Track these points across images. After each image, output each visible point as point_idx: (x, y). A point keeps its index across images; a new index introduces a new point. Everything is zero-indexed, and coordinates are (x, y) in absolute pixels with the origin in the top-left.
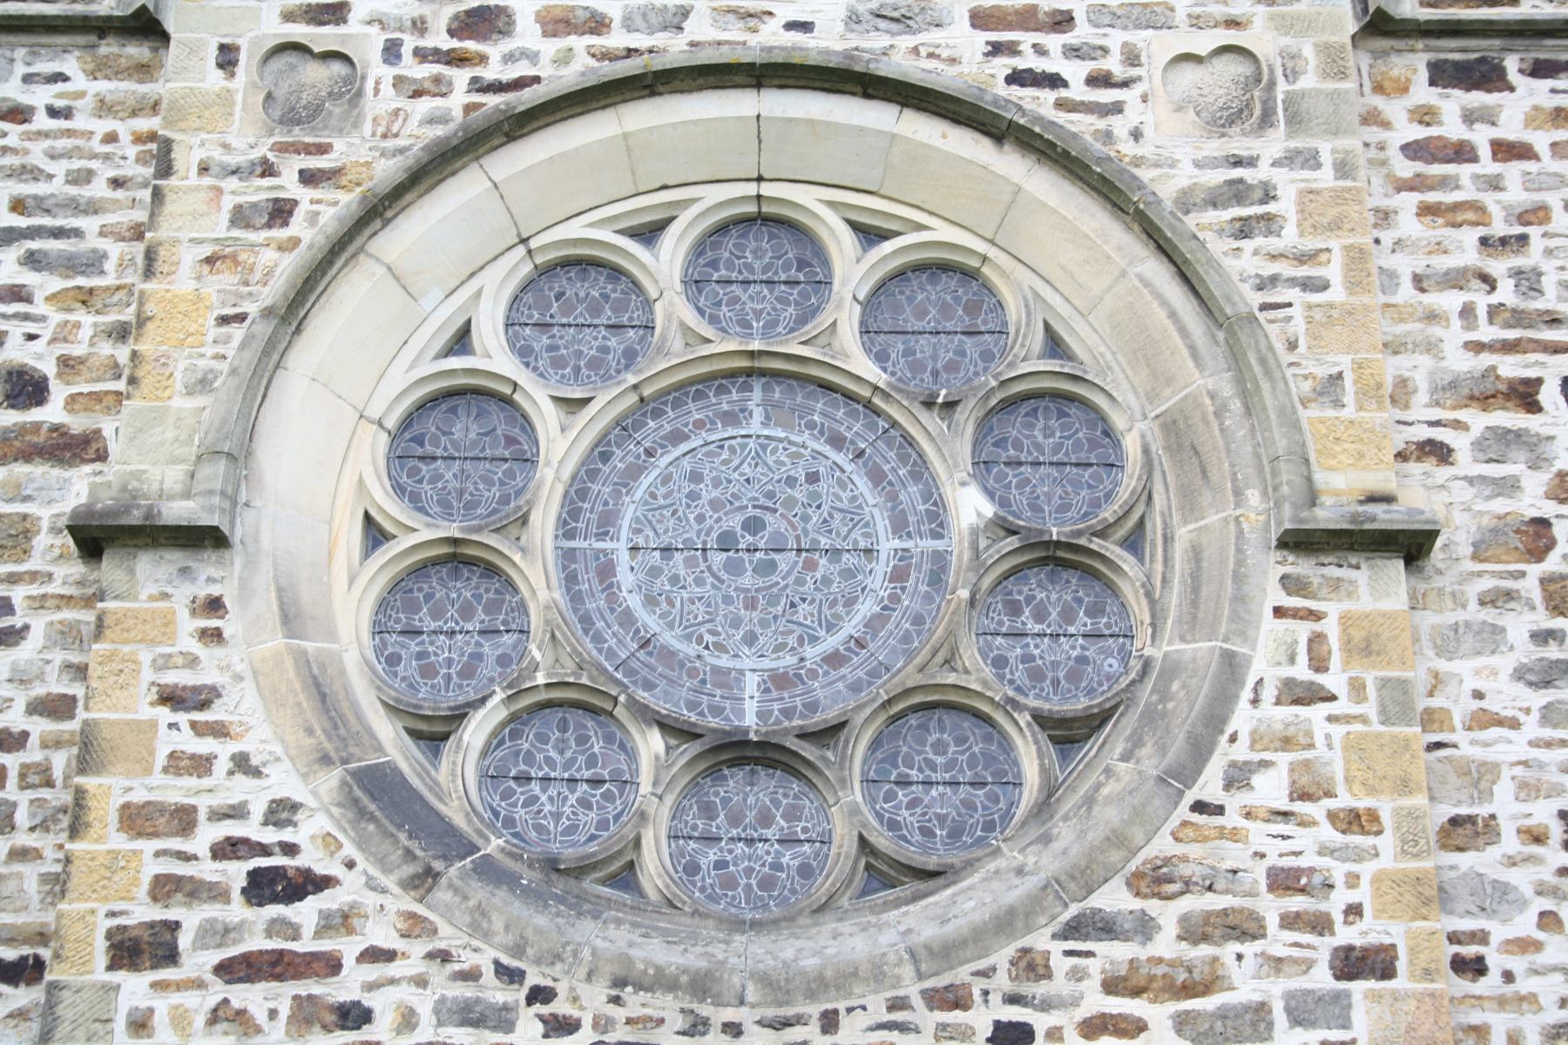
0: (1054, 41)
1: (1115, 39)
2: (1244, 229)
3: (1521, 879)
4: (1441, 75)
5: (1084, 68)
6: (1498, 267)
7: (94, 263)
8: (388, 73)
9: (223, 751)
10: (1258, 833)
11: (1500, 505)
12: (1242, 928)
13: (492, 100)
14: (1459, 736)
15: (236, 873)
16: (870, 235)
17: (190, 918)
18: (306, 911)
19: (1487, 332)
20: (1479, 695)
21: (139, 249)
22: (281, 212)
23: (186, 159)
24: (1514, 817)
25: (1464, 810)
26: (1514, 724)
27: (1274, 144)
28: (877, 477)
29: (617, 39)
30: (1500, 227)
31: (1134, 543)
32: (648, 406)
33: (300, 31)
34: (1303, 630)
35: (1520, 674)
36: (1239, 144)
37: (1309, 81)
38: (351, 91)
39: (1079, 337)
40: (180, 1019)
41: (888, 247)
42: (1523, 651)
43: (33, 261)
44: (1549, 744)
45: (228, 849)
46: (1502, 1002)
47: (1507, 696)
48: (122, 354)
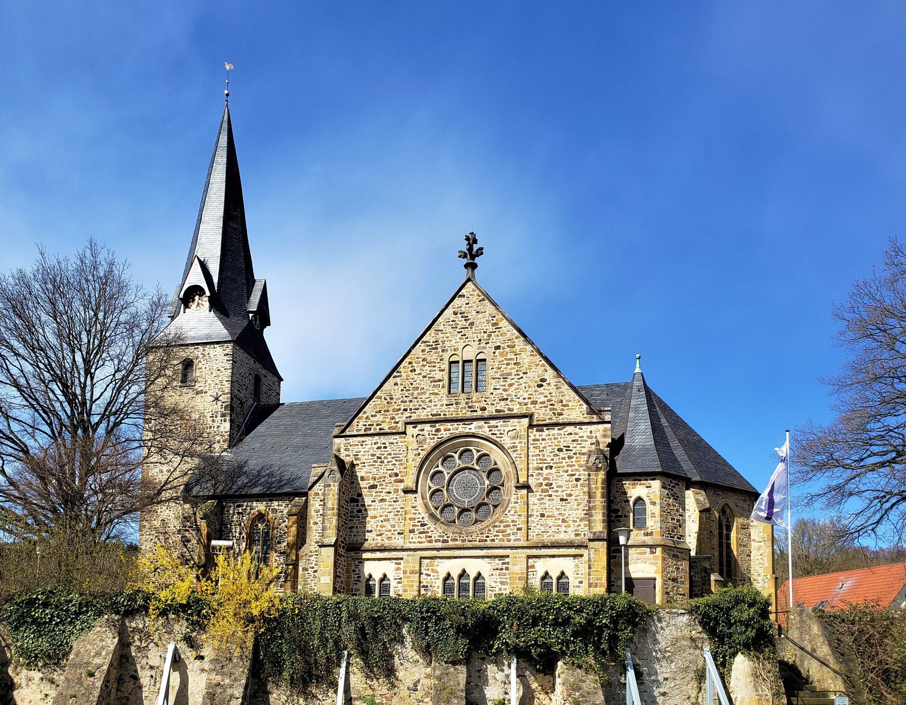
0: (496, 429)
1: (502, 428)
2: (514, 451)
4: (537, 431)
5: (499, 432)
6: (540, 454)
7: (402, 460)
8: (428, 437)
9: (417, 512)
10: (511, 517)
11: (538, 481)
13: (440, 440)
15: (419, 524)
16: (478, 451)
17: (416, 528)
18: (426, 527)
19: (539, 462)
21: (406, 459)
22: (419, 454)
27: (518, 441)
28: (478, 479)
29: (452, 431)
30: (541, 449)
31: (503, 486)
33: (420, 432)
34: (516, 496)
35: (538, 499)
36: (514, 441)
37: (522, 433)
38: (425, 440)
39: (498, 462)
40: (415, 538)
41: (479, 453)
42: (538, 497)
43: (396, 460)
45: (419, 522)
47: (537, 502)
48: (405, 470)
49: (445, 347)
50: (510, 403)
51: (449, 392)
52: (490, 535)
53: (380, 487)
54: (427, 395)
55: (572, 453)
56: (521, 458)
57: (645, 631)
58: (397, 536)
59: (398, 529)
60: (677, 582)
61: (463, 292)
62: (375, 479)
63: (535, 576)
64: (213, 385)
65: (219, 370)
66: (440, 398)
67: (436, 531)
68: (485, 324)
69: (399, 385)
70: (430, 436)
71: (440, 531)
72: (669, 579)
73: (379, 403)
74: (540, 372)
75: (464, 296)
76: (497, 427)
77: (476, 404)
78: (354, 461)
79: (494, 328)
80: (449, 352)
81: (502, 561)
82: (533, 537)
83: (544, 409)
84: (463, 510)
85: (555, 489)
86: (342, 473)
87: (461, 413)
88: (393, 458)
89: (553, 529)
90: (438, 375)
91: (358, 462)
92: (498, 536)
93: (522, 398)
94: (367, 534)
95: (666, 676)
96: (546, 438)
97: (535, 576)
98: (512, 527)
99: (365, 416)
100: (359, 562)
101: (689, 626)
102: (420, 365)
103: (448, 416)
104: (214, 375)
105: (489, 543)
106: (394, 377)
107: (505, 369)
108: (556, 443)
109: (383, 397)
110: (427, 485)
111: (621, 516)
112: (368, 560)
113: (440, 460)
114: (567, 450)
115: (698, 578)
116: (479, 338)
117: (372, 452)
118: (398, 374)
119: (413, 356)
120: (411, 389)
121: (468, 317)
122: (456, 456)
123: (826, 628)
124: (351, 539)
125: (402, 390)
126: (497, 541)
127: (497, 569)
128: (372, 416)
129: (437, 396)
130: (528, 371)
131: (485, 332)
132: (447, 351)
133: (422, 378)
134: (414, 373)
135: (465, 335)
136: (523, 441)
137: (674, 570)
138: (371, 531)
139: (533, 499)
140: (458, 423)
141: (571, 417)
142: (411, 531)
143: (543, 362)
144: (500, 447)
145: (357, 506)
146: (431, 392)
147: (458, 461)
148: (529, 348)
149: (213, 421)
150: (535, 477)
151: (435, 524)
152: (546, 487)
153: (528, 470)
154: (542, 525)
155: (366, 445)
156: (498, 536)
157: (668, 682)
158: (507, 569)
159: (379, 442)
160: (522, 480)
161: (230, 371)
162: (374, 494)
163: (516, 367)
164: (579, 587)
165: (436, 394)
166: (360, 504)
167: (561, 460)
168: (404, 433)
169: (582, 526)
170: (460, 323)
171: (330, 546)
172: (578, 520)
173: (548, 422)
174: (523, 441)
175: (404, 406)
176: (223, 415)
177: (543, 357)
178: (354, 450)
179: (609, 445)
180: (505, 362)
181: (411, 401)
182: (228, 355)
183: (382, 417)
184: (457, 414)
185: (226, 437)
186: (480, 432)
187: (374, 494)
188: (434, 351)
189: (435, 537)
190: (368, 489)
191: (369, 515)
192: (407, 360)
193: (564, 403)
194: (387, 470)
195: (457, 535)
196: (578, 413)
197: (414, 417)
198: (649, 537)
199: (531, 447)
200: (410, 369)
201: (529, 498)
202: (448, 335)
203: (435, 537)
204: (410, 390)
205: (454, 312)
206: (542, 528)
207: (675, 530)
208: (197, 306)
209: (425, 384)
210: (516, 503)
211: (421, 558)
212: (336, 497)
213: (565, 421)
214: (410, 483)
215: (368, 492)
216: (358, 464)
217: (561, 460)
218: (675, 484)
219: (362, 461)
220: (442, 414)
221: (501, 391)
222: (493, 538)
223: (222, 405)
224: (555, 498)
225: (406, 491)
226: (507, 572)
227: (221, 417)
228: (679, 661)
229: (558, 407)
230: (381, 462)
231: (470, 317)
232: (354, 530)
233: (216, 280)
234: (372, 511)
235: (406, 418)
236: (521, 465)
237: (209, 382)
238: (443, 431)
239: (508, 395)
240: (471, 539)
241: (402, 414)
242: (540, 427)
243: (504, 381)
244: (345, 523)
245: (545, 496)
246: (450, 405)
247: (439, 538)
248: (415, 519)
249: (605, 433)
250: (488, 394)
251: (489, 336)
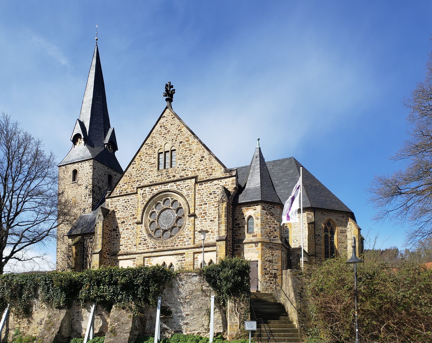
0: (179, 186)
1: (183, 185)
5: (181, 188)
6: (201, 197)
7: (136, 208)
9: (142, 234)
11: (200, 212)
12: (185, 237)
15: (143, 240)
17: (142, 242)
18: (146, 241)
19: (200, 201)
23: (139, 201)
28: (173, 214)
29: (159, 190)
30: (202, 195)
31: (184, 216)
32: (162, 211)
33: (144, 192)
34: (189, 221)
36: (188, 192)
38: (146, 196)
41: (173, 200)
42: (200, 220)
43: (133, 208)
45: (143, 239)
47: (199, 223)
49: (156, 145)
50: (187, 172)
51: (158, 169)
52: (176, 243)
53: (126, 222)
54: (148, 172)
55: (216, 195)
56: (191, 200)
57: (171, 286)
58: (134, 247)
59: (134, 243)
60: (272, 263)
61: (165, 114)
62: (124, 218)
63: (197, 263)
64: (85, 181)
65: (87, 173)
66: (154, 173)
67: (151, 242)
68: (175, 130)
69: (135, 168)
70: (148, 193)
71: (153, 243)
72: (266, 261)
73: (126, 179)
74: (201, 153)
75: (165, 117)
76: (180, 185)
77: (171, 174)
78: (115, 210)
79: (179, 132)
80: (158, 148)
81: (182, 256)
82: (197, 242)
83: (203, 173)
84: (165, 231)
85: (208, 215)
86: (104, 216)
87: (163, 180)
88: (132, 207)
90: (153, 161)
91: (116, 210)
92: (180, 243)
93: (193, 168)
94: (121, 247)
95: (187, 313)
96: (204, 188)
97: (197, 263)
98: (186, 238)
99: (119, 186)
100: (117, 261)
101: (200, 282)
102: (145, 156)
103: (157, 182)
104: (85, 176)
105: (175, 247)
106: (133, 164)
107: (185, 154)
108: (209, 190)
109: (128, 176)
110: (147, 219)
111: (241, 227)
112: (121, 260)
113: (154, 206)
114: (214, 194)
115: (295, 260)
116: (172, 139)
117: (123, 205)
118: (134, 163)
119: (141, 152)
120: (140, 170)
121: (167, 128)
122: (162, 203)
123: (296, 281)
124: (113, 250)
125: (136, 171)
126: (179, 246)
127: (180, 261)
128: (123, 186)
129: (153, 172)
130: (195, 153)
131: (175, 135)
132: (157, 147)
133: (145, 164)
134: (141, 161)
135: (165, 138)
136: (192, 191)
137: (270, 255)
138: (122, 245)
139: (197, 222)
140: (162, 185)
141: (216, 175)
142: (140, 244)
143: (203, 147)
144: (182, 195)
145: (116, 233)
146: (150, 170)
147: (163, 206)
148: (196, 140)
149: (85, 198)
150: (198, 210)
151: (150, 239)
152: (203, 215)
153: (195, 206)
155: (120, 201)
156: (180, 243)
157: (189, 317)
158: (184, 260)
159: (126, 199)
160: (192, 212)
161: (92, 173)
162: (124, 226)
163: (190, 152)
165: (152, 171)
166: (117, 231)
167: (211, 199)
168: (137, 193)
170: (163, 132)
171: (97, 253)
173: (205, 179)
174: (192, 191)
175: (137, 179)
176: (89, 195)
177: (203, 144)
178: (115, 204)
179: (235, 188)
180: (185, 150)
181: (140, 176)
182: (91, 165)
183: (127, 186)
184: (162, 181)
185: (91, 206)
186: (172, 189)
187: (124, 226)
188: (151, 148)
189: (150, 246)
190: (121, 224)
191: (121, 237)
192: (139, 154)
193: (213, 168)
194: (129, 213)
195: (161, 244)
196: (220, 173)
197: (142, 184)
198: (255, 238)
199: (197, 194)
200: (140, 159)
201: (195, 222)
202: (158, 139)
203: (150, 246)
204: (140, 170)
205: (160, 126)
207: (272, 233)
208: (79, 143)
209: (147, 166)
210: (188, 224)
211: (144, 257)
212: (102, 228)
213: (213, 178)
214: (139, 219)
215: (121, 225)
216: (116, 211)
217: (211, 199)
218: (272, 207)
219: (118, 210)
220: (155, 181)
221: (182, 166)
222: (177, 244)
223: (89, 190)
224: (208, 220)
225: (138, 223)
226: (184, 262)
227: (89, 196)
228: (196, 304)
229: (210, 170)
230: (126, 209)
231: (168, 128)
232: (115, 245)
233: (88, 130)
234: (123, 235)
235: (138, 185)
236: (191, 204)
237: (84, 180)
238: (154, 190)
239: (186, 167)
240: (167, 246)
241: (136, 183)
242: (201, 183)
243: (184, 160)
244: (108, 241)
245: (203, 219)
246: (158, 176)
247: (152, 246)
248: (141, 238)
249: (233, 182)
250: (176, 168)
251: (177, 136)
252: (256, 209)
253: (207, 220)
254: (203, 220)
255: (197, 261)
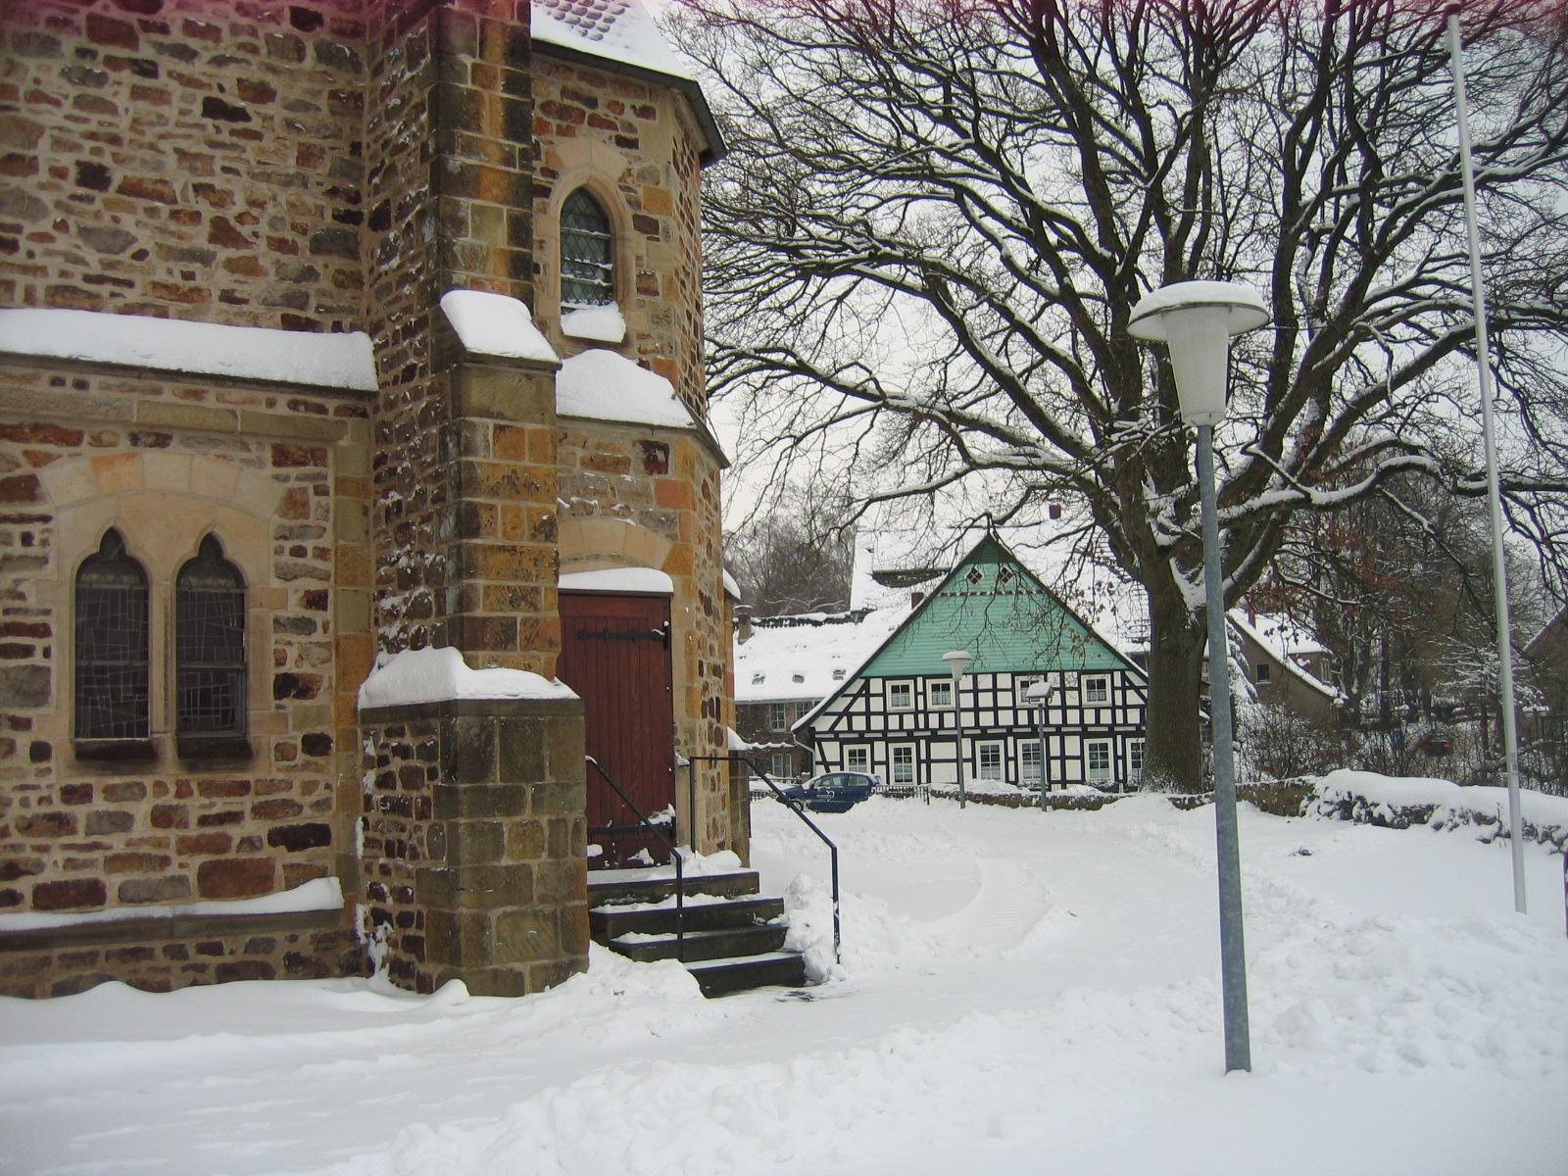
3: (47, 198)
14: (21, 104)
20: (37, 81)
24: (49, 159)
25: (18, 151)
26: (57, 103)
35: (65, 74)
44: (76, 119)
46: (25, 269)
63: (34, 550)
85: (177, 36)
89: (162, 271)
154: (85, 232)
164: (304, 626)
169: (325, 283)
172: (303, 242)
206: (94, 260)
224: (175, 88)
245: (113, 63)
252: (631, 144)
253: (163, 81)
254: (113, 76)
255: (31, 519)
